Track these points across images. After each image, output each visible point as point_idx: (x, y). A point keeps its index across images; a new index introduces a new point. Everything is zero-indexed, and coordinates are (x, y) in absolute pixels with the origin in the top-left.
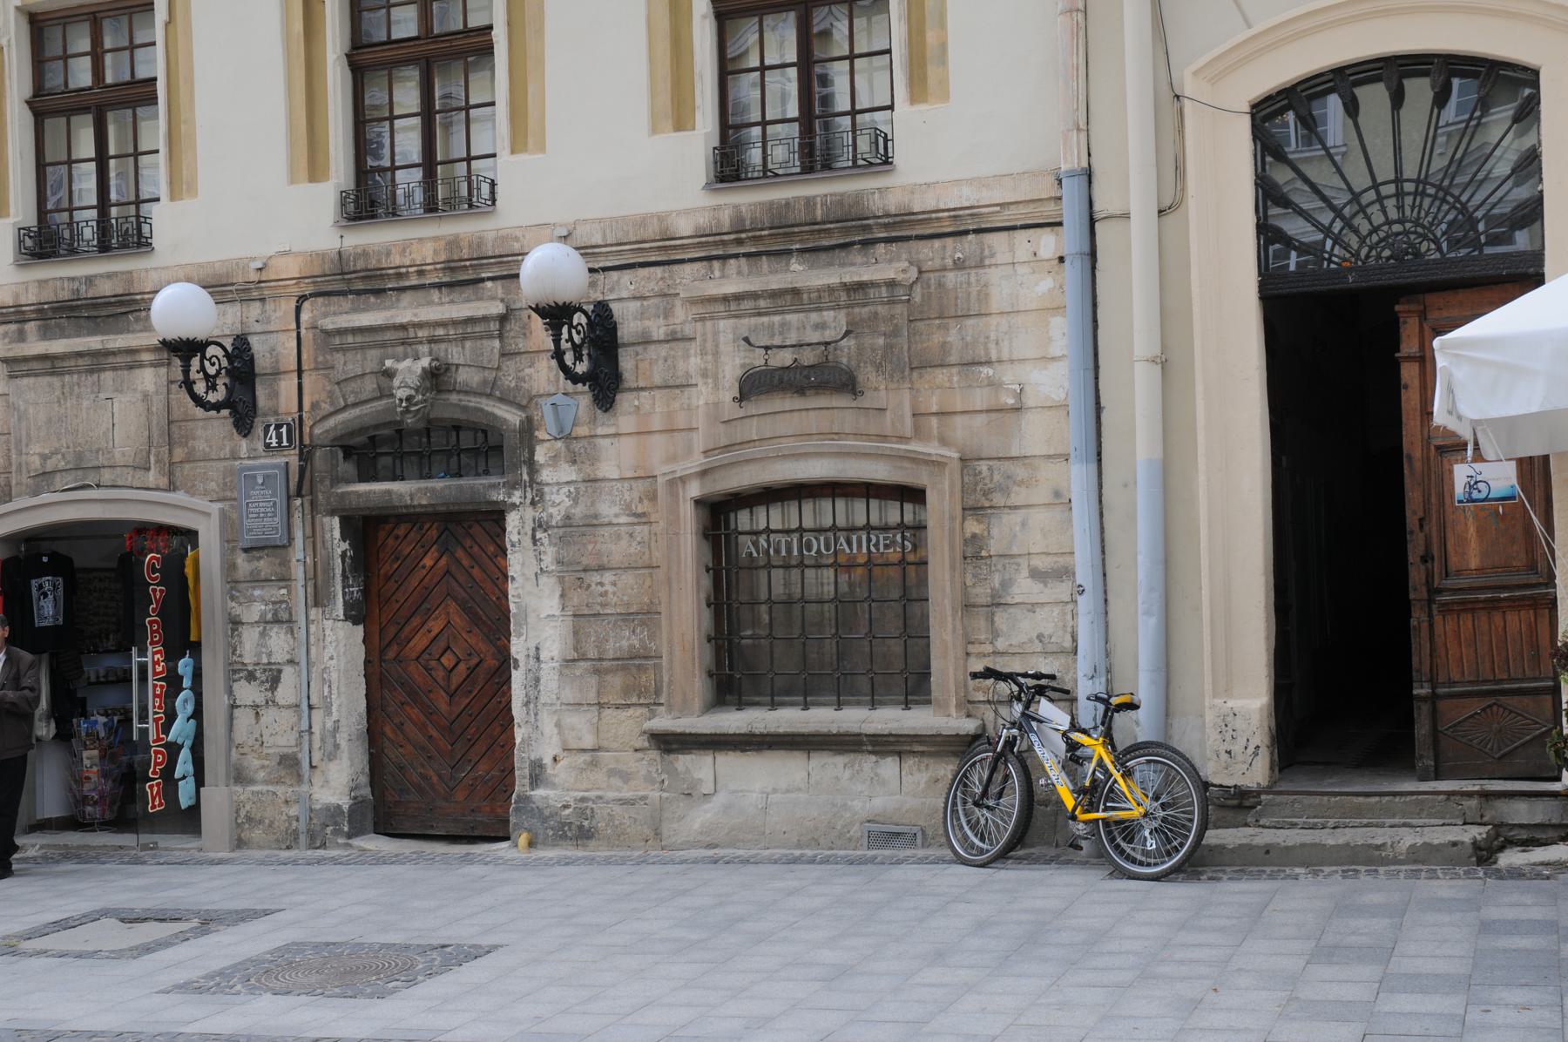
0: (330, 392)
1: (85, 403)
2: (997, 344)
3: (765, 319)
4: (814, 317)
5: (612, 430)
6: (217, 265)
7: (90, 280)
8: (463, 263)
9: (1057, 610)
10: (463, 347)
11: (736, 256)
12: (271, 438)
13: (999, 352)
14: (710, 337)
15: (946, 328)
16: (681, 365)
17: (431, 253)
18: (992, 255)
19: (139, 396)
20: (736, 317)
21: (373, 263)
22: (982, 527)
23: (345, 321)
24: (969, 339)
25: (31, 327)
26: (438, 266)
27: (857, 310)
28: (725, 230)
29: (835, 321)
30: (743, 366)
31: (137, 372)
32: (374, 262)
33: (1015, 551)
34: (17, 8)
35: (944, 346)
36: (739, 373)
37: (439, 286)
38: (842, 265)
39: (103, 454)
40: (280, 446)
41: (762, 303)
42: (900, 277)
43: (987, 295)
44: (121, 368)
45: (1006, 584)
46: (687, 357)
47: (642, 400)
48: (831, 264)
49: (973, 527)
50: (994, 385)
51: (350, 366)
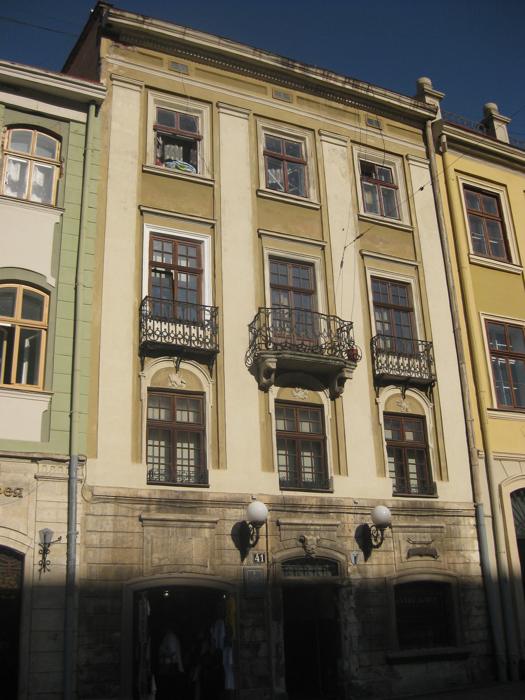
0: (278, 544)
1: (180, 540)
2: (463, 546)
3: (411, 534)
4: (423, 534)
5: (370, 563)
6: (237, 495)
7: (184, 493)
8: (325, 506)
10: (325, 533)
11: (402, 515)
12: (257, 559)
13: (464, 548)
14: (397, 537)
16: (389, 545)
17: (315, 502)
18: (461, 523)
19: (204, 539)
20: (403, 532)
21: (295, 502)
23: (288, 521)
24: (457, 544)
25: (153, 507)
26: (317, 506)
27: (433, 533)
28: (400, 507)
29: (427, 537)
30: (407, 547)
31: (202, 529)
32: (296, 502)
34: (148, 387)
35: (452, 546)
36: (405, 548)
37: (316, 513)
39: (188, 559)
40: (260, 562)
41: (410, 529)
42: (443, 525)
43: (460, 533)
44: (196, 527)
46: (390, 543)
47: (379, 554)
50: (464, 556)
51: (286, 536)
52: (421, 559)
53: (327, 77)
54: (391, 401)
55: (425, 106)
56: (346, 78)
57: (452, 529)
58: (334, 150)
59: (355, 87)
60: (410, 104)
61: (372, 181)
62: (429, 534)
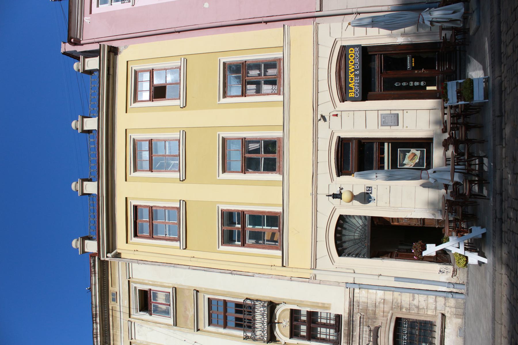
2: (373, 301)
3: (364, 341)
4: (364, 332)
9: (420, 297)
13: (374, 301)
15: (369, 310)
18: (358, 300)
22: (404, 308)
24: (371, 306)
27: (364, 324)
29: (366, 329)
33: (409, 303)
35: (371, 310)
38: (356, 326)
41: (361, 341)
45: (415, 305)
48: (355, 328)
49: (404, 310)
50: (380, 303)
52: (379, 337)
53: (97, 334)
54: (283, 332)
55: (93, 266)
56: (93, 323)
57: (362, 308)
58: (139, 332)
59: (97, 315)
60: (94, 276)
61: (150, 307)
62: (364, 327)
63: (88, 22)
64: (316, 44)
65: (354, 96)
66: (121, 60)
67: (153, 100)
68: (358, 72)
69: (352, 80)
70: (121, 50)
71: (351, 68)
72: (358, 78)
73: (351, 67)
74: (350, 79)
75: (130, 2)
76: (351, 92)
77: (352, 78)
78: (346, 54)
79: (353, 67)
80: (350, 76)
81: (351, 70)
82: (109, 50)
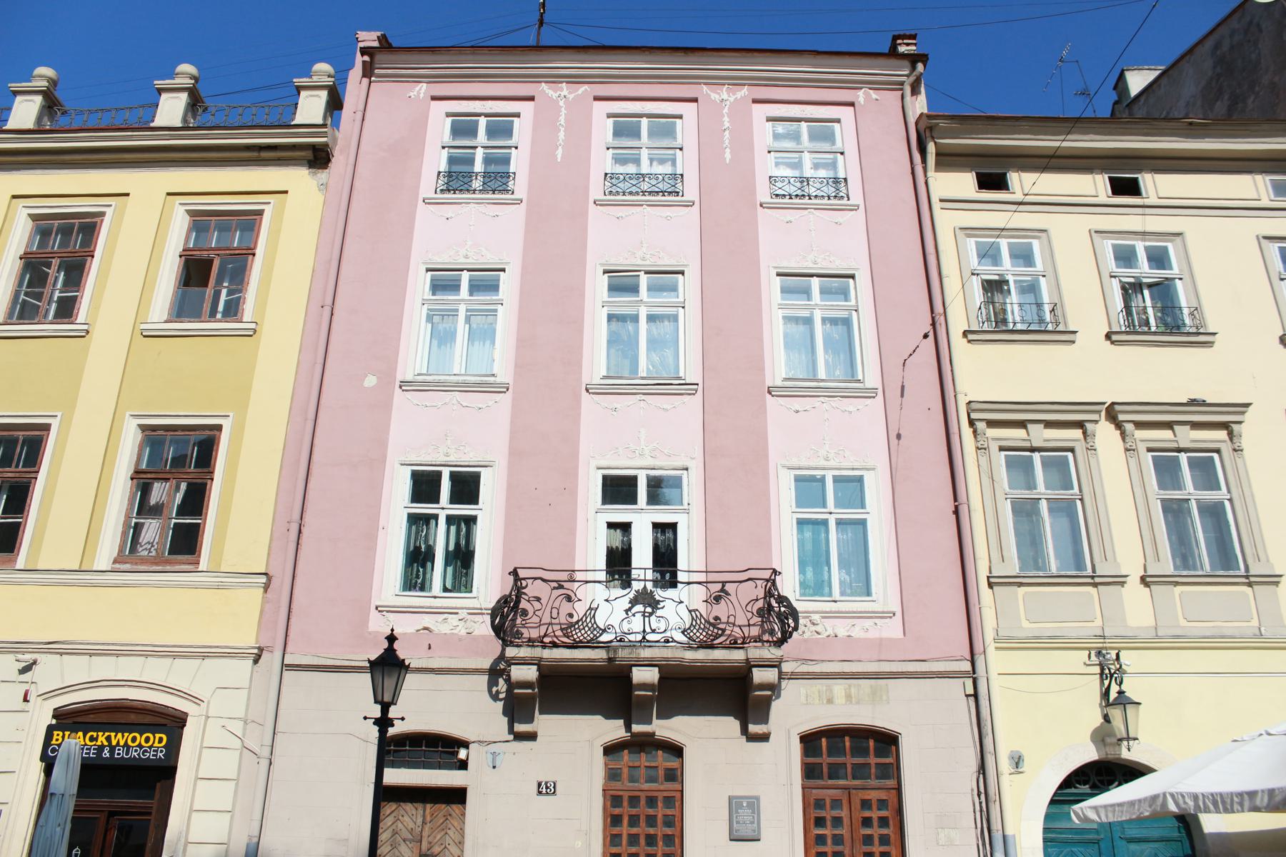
63: (411, 94)
64: (204, 654)
65: (52, 743)
66: (297, 178)
67: (183, 258)
68: (108, 755)
69: (92, 739)
70: (319, 175)
71: (119, 738)
72: (93, 754)
73: (123, 736)
74: (95, 734)
75: (436, 193)
76: (63, 737)
77: (96, 739)
78: (165, 725)
79: (122, 743)
80: (69, 733)
81: (116, 736)
82: (317, 147)
